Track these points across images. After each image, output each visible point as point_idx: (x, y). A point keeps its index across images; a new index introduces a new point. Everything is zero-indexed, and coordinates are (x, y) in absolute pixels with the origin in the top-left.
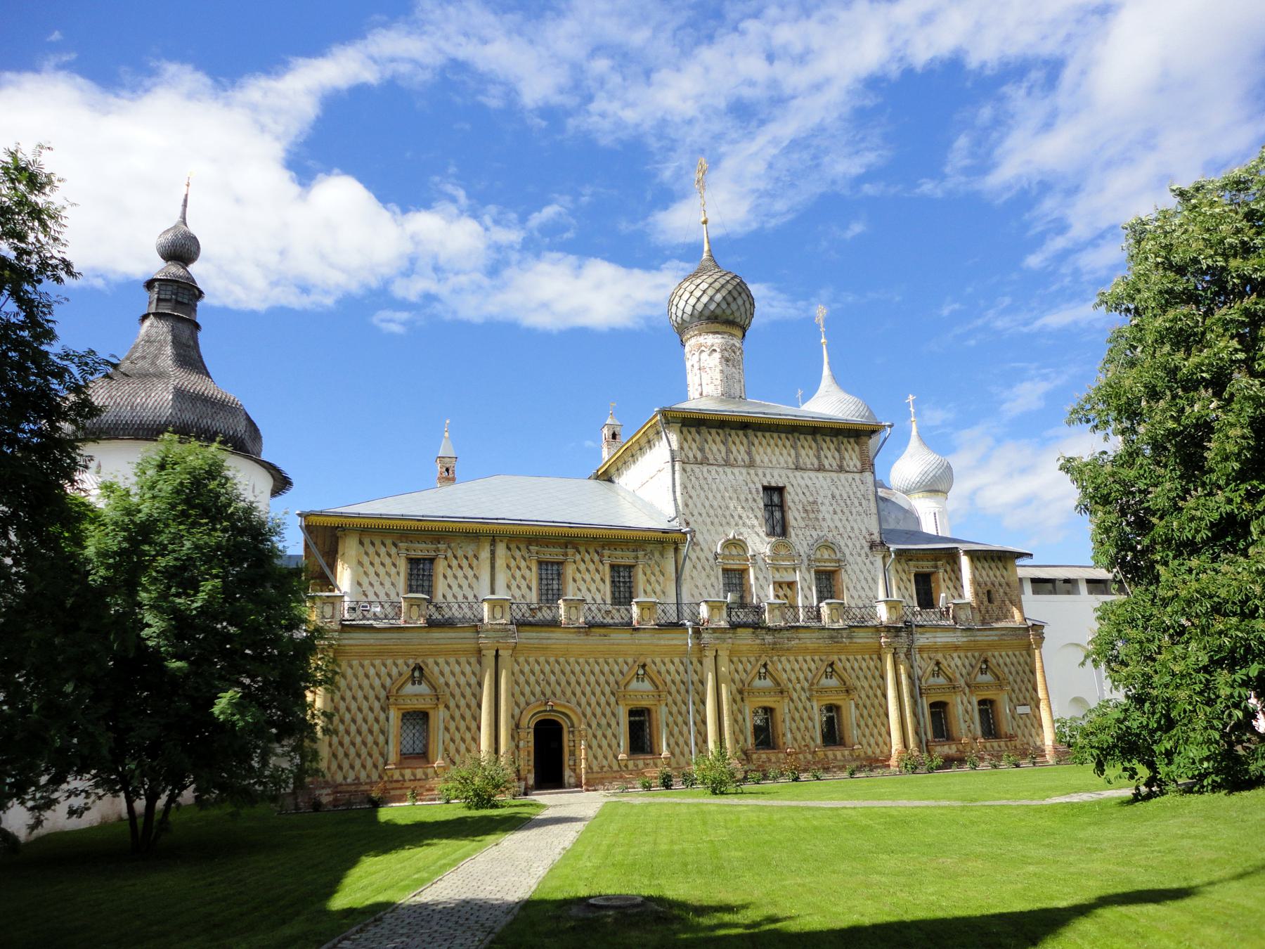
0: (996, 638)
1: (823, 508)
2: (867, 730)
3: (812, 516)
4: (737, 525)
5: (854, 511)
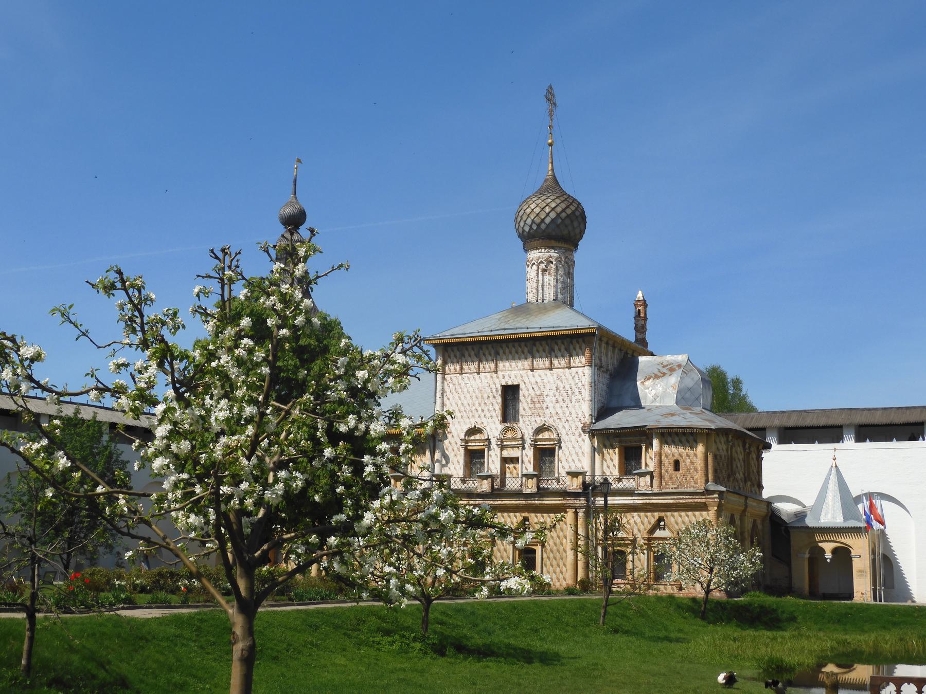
0: (672, 501)
1: (547, 399)
2: (551, 568)
3: (538, 405)
4: (479, 417)
5: (574, 399)
